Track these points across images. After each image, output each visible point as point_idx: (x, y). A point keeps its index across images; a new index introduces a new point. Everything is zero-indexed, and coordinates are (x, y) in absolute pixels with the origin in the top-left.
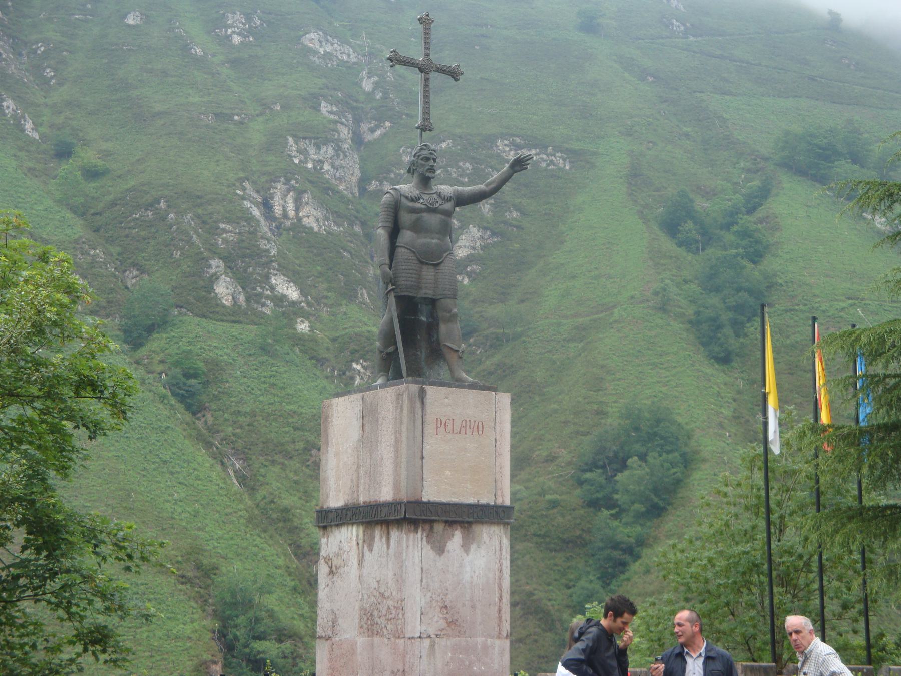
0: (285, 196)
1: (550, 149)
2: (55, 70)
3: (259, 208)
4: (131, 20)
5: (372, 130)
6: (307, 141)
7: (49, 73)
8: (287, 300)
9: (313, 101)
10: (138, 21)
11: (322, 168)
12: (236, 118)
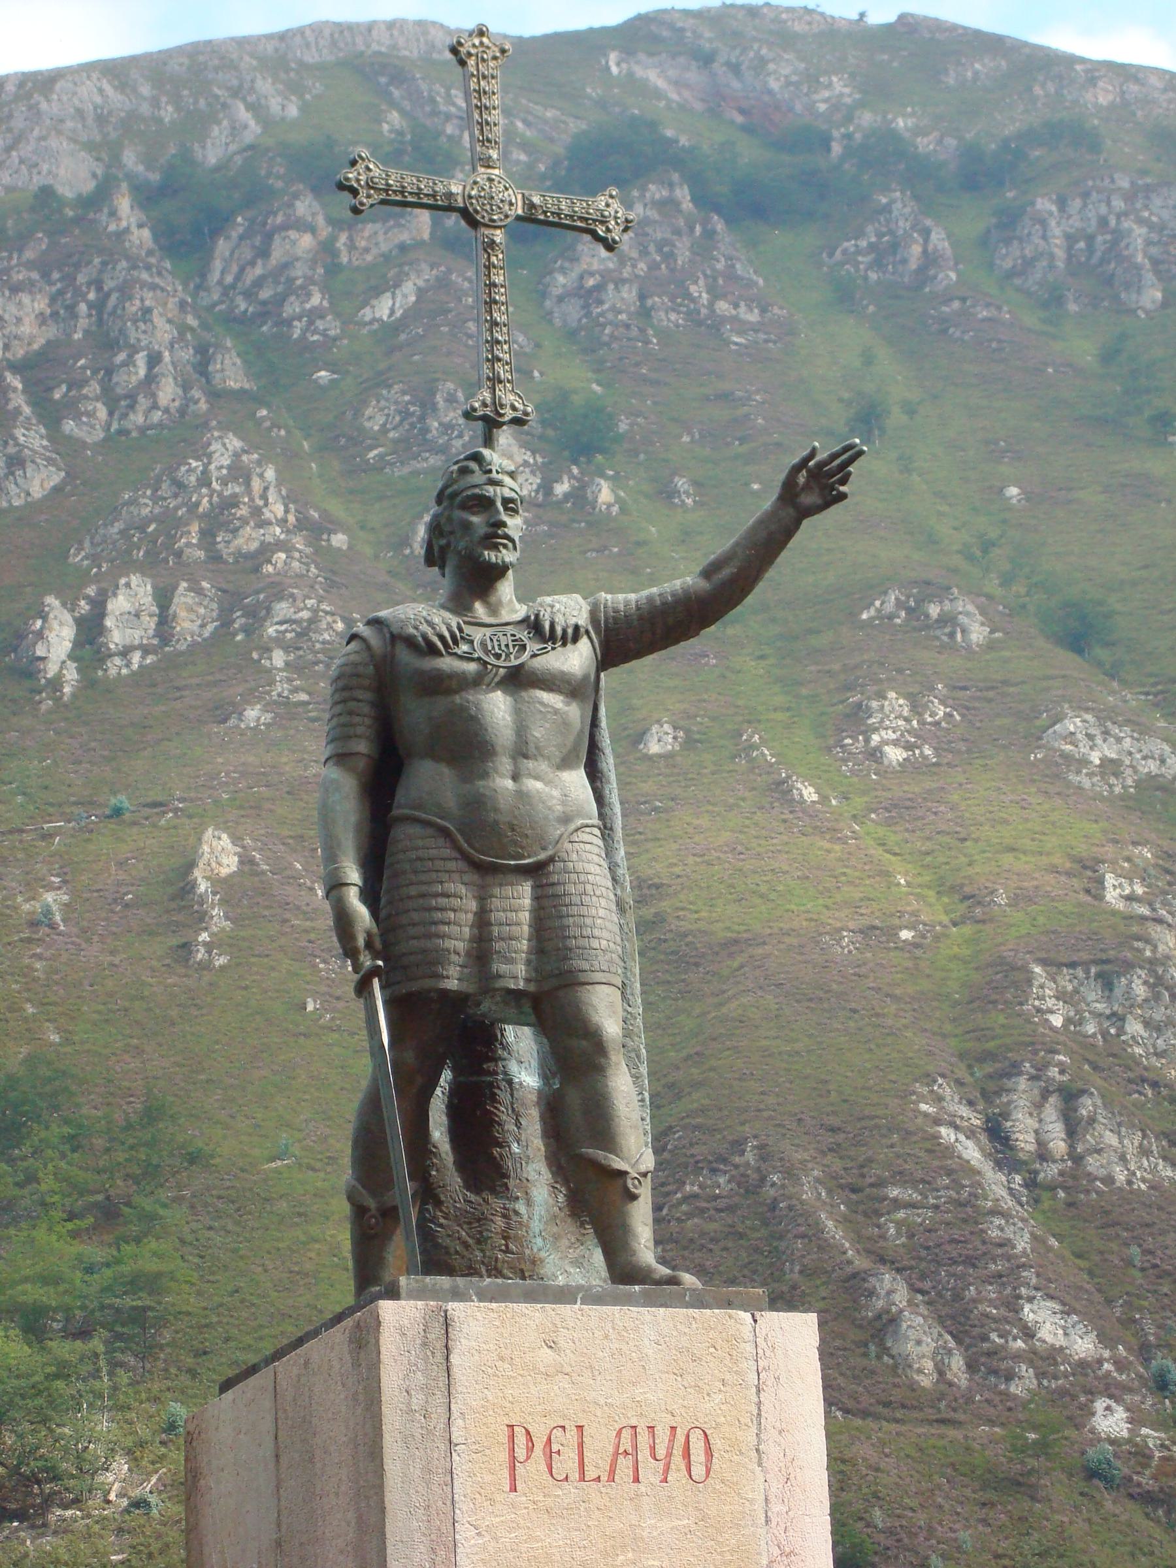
0: (1039, 1106)
3: (978, 1143)
6: (1080, 972)
8: (1067, 1359)
11: (1121, 1031)
12: (905, 935)
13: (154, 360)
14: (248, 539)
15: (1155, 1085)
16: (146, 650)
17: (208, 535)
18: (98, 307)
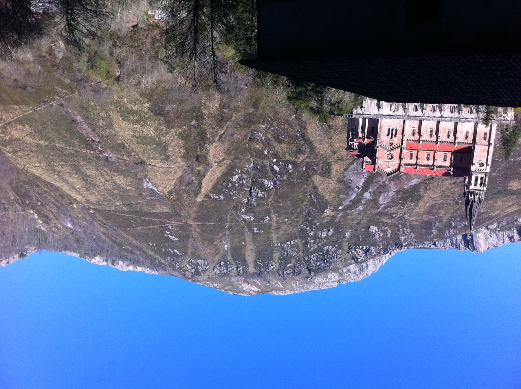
1: (213, 198)
2: (303, 209)
4: (287, 220)
5: (245, 201)
7: (304, 208)
9: (258, 205)
10: (285, 220)
13: (313, 260)
14: (312, 241)
15: (259, 187)
16: (323, 231)
17: (315, 241)
18: (316, 265)
